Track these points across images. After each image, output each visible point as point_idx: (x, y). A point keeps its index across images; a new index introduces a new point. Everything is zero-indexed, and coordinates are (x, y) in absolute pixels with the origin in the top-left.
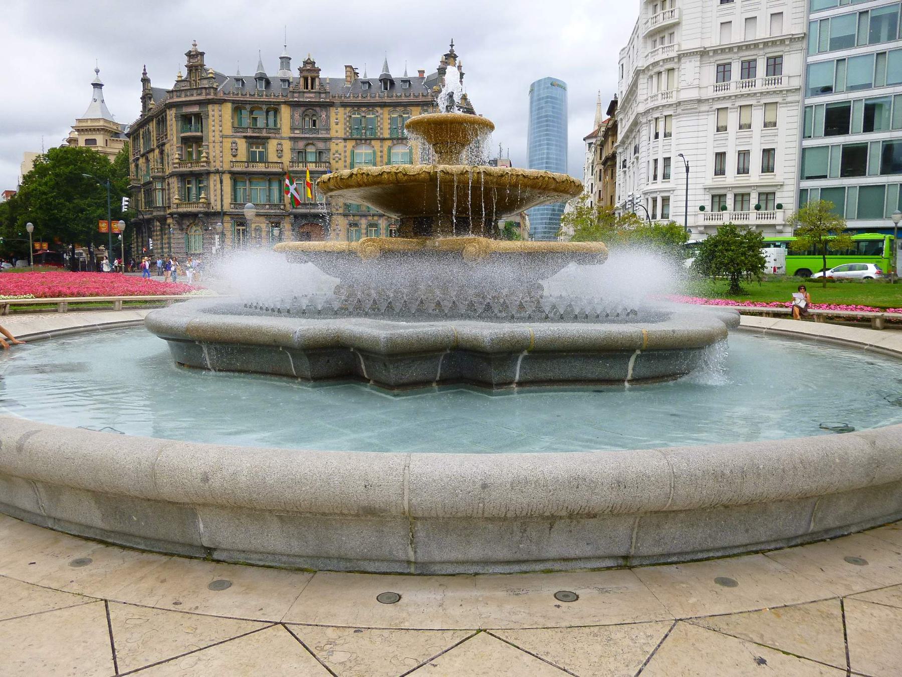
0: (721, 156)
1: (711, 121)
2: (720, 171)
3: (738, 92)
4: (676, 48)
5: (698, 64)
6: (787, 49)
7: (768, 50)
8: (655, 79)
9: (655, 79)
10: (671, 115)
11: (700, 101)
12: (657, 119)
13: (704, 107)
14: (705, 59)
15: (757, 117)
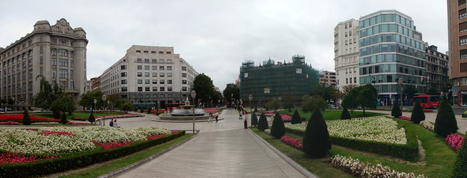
0: (347, 79)
1: (345, 71)
2: (347, 83)
3: (353, 64)
4: (338, 55)
5: (341, 59)
6: (357, 55)
7: (349, 56)
8: (337, 61)
9: (337, 61)
10: (351, 68)
11: (342, 67)
12: (338, 70)
13: (343, 68)
14: (343, 58)
15: (352, 70)
